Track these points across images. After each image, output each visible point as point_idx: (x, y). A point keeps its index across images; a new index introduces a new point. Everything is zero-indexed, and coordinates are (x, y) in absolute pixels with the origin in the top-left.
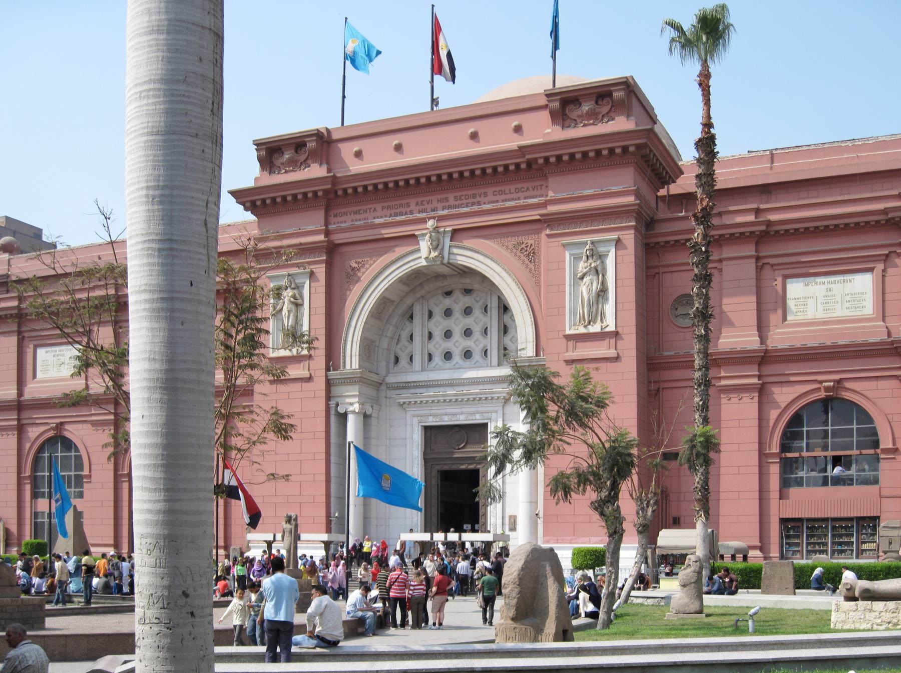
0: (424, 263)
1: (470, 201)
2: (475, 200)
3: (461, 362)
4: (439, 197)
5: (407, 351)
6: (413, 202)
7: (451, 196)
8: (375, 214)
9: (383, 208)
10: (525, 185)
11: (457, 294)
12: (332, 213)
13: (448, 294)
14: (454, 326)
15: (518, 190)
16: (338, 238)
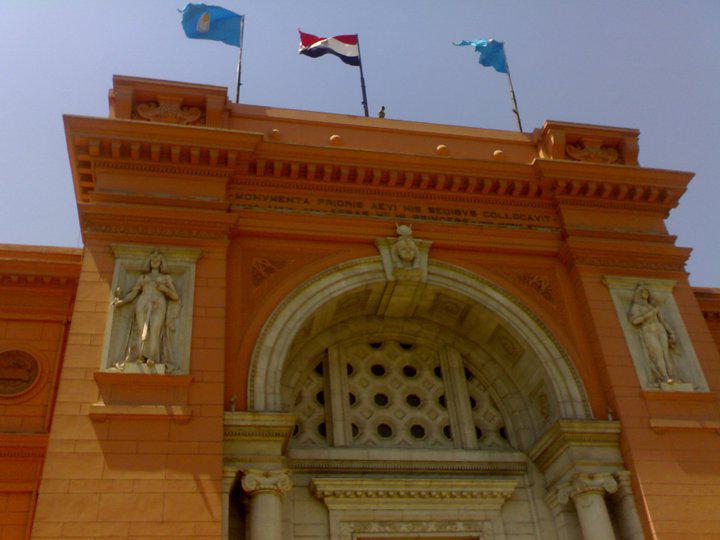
0: (391, 278)
1: (455, 216)
2: (462, 216)
5: (315, 416)
9: (321, 201)
13: (376, 346)
15: (516, 217)
16: (249, 224)
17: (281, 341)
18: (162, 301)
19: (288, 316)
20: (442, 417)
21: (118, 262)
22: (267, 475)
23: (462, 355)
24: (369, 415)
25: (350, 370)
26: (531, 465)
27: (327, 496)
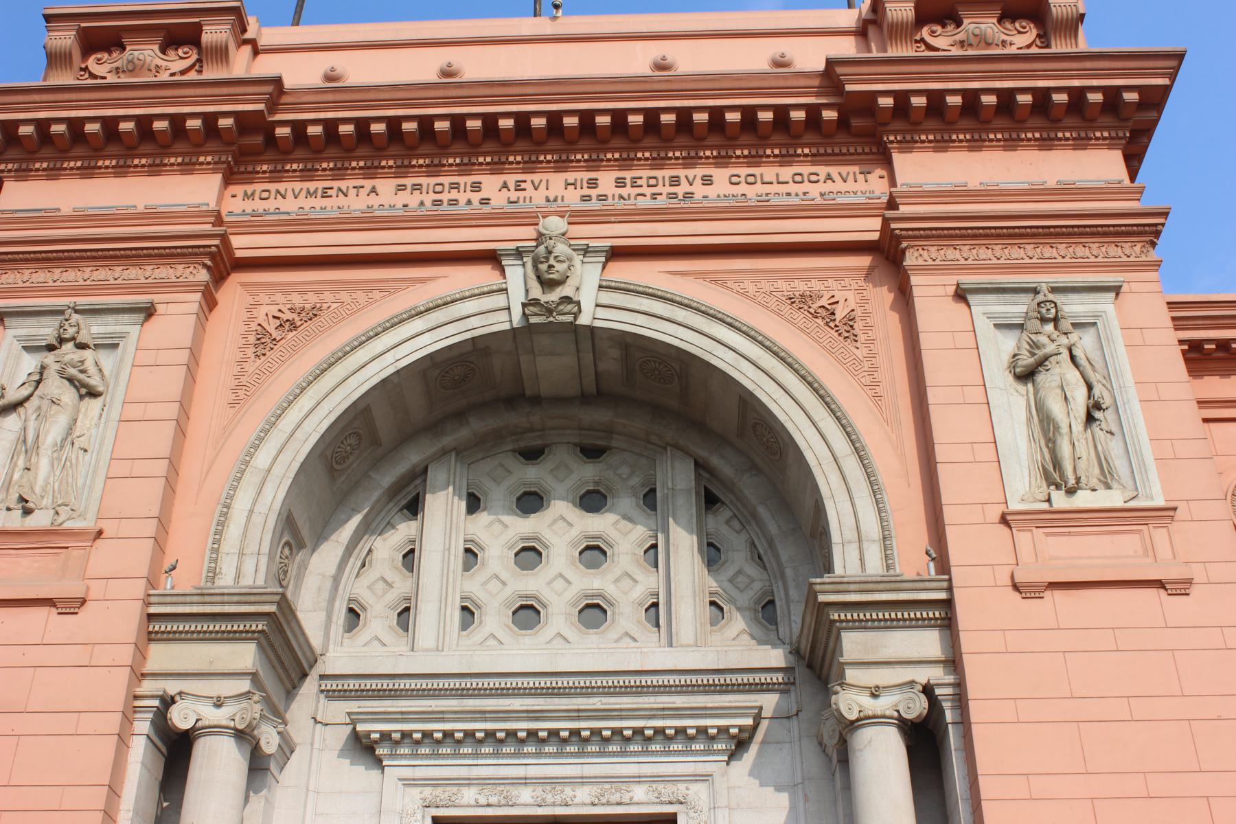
3: (569, 633)
4: (571, 176)
6: (491, 184)
7: (606, 180)
8: (374, 201)
10: (823, 170)
11: (562, 455)
12: (239, 190)
13: (532, 455)
14: (547, 535)
15: (797, 179)
17: (285, 457)
18: (68, 395)
19: (306, 410)
20: (647, 582)
21: (10, 333)
22: (218, 704)
23: (697, 464)
24: (498, 583)
25: (474, 503)
26: (801, 673)
27: (376, 742)
